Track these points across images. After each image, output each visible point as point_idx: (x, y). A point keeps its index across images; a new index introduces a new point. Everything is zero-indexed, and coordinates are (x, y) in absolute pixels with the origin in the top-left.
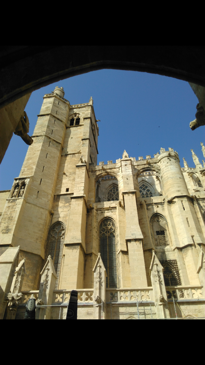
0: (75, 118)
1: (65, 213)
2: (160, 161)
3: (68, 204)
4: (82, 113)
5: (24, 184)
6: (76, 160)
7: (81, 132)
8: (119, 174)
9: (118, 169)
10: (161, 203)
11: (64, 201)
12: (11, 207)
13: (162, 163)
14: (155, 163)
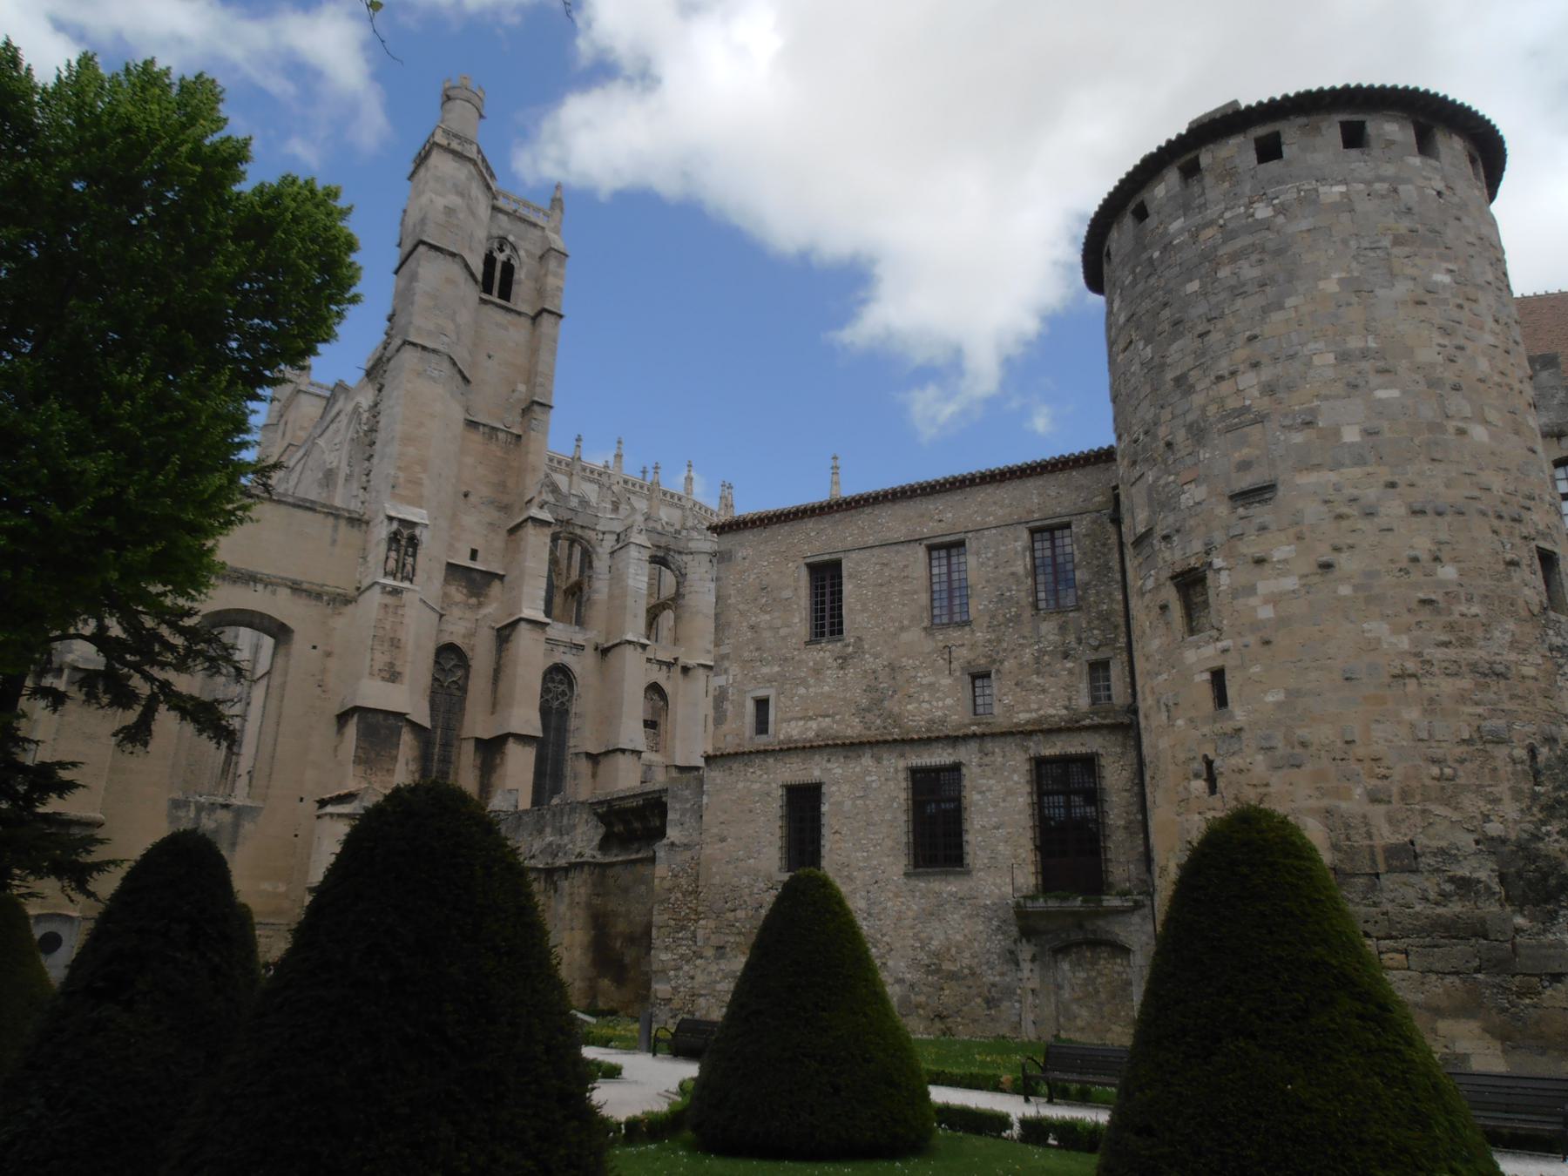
0: (501, 257)
1: (469, 625)
2: (692, 553)
3: (473, 601)
4: (526, 251)
5: (413, 542)
6: (499, 454)
8: (599, 550)
9: (600, 536)
10: (670, 663)
11: (466, 587)
12: (391, 610)
14: (680, 553)
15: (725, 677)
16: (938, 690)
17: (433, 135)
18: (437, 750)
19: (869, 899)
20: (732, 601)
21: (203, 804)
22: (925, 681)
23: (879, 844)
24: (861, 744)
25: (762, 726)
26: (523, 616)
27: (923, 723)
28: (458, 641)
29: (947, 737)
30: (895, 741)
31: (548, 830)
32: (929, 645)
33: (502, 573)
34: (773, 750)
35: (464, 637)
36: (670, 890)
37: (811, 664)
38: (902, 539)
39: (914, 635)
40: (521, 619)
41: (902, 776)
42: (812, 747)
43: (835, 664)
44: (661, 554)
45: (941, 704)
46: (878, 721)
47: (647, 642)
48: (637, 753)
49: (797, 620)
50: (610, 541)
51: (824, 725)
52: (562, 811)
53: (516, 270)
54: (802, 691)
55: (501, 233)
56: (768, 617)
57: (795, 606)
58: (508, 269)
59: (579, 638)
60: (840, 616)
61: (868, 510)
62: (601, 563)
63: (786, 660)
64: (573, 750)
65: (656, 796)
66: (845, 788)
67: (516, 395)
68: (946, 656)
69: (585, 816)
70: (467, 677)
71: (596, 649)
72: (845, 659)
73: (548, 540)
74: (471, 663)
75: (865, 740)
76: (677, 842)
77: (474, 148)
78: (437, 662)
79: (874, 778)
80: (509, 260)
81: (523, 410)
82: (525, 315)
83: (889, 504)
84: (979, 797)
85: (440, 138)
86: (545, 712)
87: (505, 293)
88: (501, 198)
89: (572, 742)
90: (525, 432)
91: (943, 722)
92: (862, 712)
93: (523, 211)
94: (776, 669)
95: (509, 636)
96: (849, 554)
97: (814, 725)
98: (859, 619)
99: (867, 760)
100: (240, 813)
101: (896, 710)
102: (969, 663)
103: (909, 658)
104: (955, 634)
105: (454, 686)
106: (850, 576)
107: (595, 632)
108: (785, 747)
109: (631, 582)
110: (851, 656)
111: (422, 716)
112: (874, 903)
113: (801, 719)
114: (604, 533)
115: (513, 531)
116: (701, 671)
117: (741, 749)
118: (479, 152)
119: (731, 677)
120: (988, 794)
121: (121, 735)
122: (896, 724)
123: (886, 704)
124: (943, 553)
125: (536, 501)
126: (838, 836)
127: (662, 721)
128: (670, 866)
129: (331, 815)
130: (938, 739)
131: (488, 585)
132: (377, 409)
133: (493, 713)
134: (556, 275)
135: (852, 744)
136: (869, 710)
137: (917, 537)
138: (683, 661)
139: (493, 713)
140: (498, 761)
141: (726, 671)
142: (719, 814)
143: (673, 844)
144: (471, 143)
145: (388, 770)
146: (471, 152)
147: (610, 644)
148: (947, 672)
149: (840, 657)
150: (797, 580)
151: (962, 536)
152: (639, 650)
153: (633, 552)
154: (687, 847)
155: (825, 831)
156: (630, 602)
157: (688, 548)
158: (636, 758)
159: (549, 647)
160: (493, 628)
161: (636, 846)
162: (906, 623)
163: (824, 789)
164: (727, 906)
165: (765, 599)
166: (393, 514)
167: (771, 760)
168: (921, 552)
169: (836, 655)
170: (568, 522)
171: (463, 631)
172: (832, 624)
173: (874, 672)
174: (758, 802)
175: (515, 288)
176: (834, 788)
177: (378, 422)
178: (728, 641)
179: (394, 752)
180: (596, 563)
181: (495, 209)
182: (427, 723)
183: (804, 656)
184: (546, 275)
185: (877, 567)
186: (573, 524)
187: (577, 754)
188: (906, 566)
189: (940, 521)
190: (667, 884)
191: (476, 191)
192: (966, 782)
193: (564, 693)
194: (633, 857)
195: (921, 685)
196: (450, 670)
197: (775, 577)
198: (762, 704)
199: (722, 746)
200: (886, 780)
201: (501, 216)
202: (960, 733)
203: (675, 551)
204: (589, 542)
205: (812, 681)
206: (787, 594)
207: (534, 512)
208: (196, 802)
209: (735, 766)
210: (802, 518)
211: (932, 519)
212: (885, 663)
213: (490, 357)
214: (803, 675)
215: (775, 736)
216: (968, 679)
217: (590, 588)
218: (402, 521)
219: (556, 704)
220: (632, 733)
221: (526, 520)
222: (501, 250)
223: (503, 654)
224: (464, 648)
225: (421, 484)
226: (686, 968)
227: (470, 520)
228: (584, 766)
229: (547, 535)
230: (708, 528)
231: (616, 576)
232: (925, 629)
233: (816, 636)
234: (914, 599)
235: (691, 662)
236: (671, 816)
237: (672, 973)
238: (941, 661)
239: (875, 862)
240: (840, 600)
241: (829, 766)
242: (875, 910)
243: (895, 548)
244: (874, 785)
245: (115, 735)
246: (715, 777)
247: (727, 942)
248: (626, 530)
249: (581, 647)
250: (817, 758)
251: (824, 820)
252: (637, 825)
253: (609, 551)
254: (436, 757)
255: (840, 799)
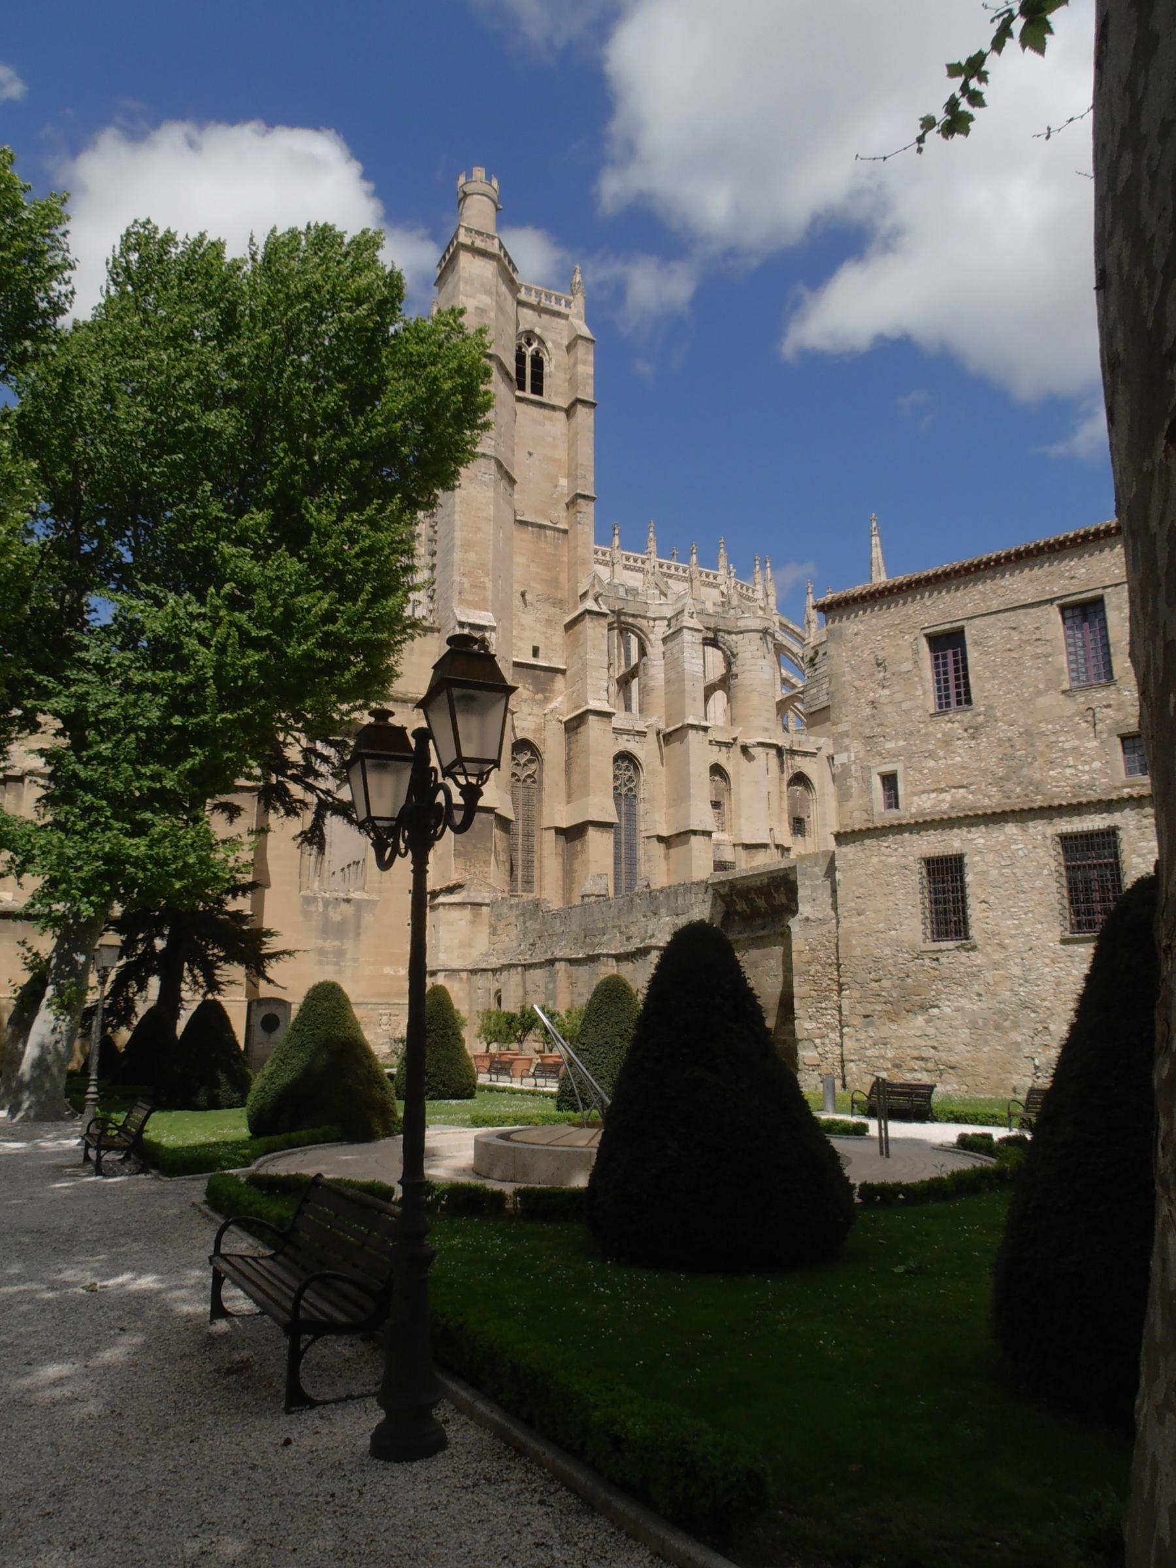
0: (529, 351)
2: (741, 632)
3: (539, 696)
4: (553, 342)
6: (548, 550)
7: (554, 438)
8: (651, 637)
9: (651, 623)
11: (533, 684)
13: (746, 641)
14: (730, 633)
15: (846, 755)
16: (1082, 755)
17: (456, 236)
18: (520, 841)
19: (1024, 966)
20: (847, 678)
21: (328, 899)
22: (1067, 745)
23: (1031, 912)
24: (1004, 812)
25: (893, 801)
26: (590, 707)
27: (1068, 789)
28: (530, 737)
29: (1100, 801)
30: (1041, 808)
31: (663, 911)
32: (1069, 707)
33: (563, 667)
34: (908, 824)
35: (536, 731)
36: (809, 963)
37: (939, 736)
38: (1030, 601)
39: (1051, 700)
40: (589, 711)
41: (1049, 841)
42: (950, 818)
43: (965, 735)
44: (711, 635)
45: (1087, 768)
46: (1018, 789)
47: (704, 723)
48: (708, 834)
49: (919, 693)
50: (661, 629)
51: (959, 796)
52: (676, 892)
53: (545, 364)
54: (931, 763)
55: (528, 327)
56: (887, 692)
57: (916, 679)
58: (538, 363)
59: (640, 727)
60: (967, 685)
61: (989, 574)
62: (656, 649)
63: (911, 733)
64: (644, 834)
65: (781, 874)
66: (990, 857)
67: (559, 489)
68: (1090, 719)
69: (701, 896)
70: (541, 770)
71: (658, 734)
72: (976, 728)
73: (605, 631)
74: (544, 756)
75: (1008, 809)
76: (811, 917)
77: (496, 242)
78: (514, 759)
79: (1020, 846)
80: (537, 353)
81: (567, 505)
82: (560, 409)
83: (1011, 565)
84: (1140, 860)
85: (464, 238)
86: (617, 797)
87: (538, 389)
88: (523, 290)
89: (642, 826)
90: (571, 526)
91: (1091, 786)
92: (998, 781)
93: (544, 303)
94: (902, 743)
95: (578, 726)
96: (970, 621)
97: (947, 797)
98: (988, 686)
99: (1011, 829)
100: (359, 905)
101: (1037, 776)
102: (1117, 723)
103: (1048, 723)
104: (1100, 696)
105: (529, 780)
106: (976, 643)
107: (655, 718)
108: (921, 820)
109: (687, 666)
110: (982, 725)
111: (507, 811)
112: (1030, 970)
113: (933, 791)
114: (654, 619)
115: (569, 626)
116: (760, 749)
117: (871, 826)
118: (501, 246)
119: (853, 755)
120: (1149, 856)
121: (300, 840)
122: (1038, 791)
123: (1025, 771)
124: (1077, 612)
125: (591, 594)
126: (984, 906)
127: (725, 801)
128: (806, 940)
129: (444, 904)
130: (1089, 804)
131: (552, 680)
132: (435, 519)
133: (568, 803)
134: (585, 363)
135: (994, 813)
136: (1006, 778)
137: (1048, 597)
138: (741, 741)
139: (568, 803)
140: (579, 848)
141: (847, 749)
142: (854, 888)
143: (807, 919)
144: (493, 238)
145: (485, 862)
146: (494, 248)
147: (671, 729)
148: (1092, 735)
149: (971, 727)
150: (916, 652)
151: (1100, 592)
152: (702, 733)
153: (687, 635)
154: (822, 921)
155: (970, 901)
156: (688, 686)
157: (738, 627)
158: (707, 838)
159: (614, 736)
160: (560, 721)
161: (759, 922)
162: (1041, 686)
163: (966, 860)
164: (871, 976)
165: (882, 674)
166: (463, 619)
167: (906, 835)
168: (1054, 613)
169: (966, 725)
170: (619, 613)
171: (532, 726)
172: (958, 694)
173: (1010, 740)
174: (892, 876)
175: (546, 382)
176: (977, 858)
177: (435, 532)
178: (845, 719)
179: (488, 845)
180: (649, 650)
181: (521, 303)
182: (511, 815)
183: (931, 729)
184: (575, 364)
185: (1005, 632)
186: (625, 614)
187: (648, 837)
188: (1037, 628)
189: (1073, 578)
190: (806, 956)
191: (504, 289)
192: (1124, 846)
193: (630, 779)
194: (761, 933)
195: (1063, 750)
196: (525, 765)
197: (893, 650)
198: (890, 780)
199: (849, 822)
200: (1035, 847)
201: (527, 313)
202: (1114, 796)
203: (724, 631)
204: (641, 630)
205: (941, 753)
206: (907, 666)
207: (590, 604)
208: (323, 898)
209: (867, 842)
210: (917, 588)
211: (1061, 576)
212: (1022, 730)
213: (530, 454)
214: (931, 747)
215: (906, 810)
216: (1118, 741)
217: (646, 675)
218: (473, 626)
219: (624, 790)
220: (701, 815)
221: (583, 614)
222: (530, 344)
223: (573, 746)
224: (536, 742)
225: (485, 588)
226: (831, 1035)
227: (527, 618)
228: (658, 848)
229: (603, 627)
230: (814, 607)
231: (673, 664)
232: (1064, 692)
233: (940, 706)
234: (1048, 663)
235: (750, 741)
236: (801, 893)
237: (818, 1041)
238: (1084, 725)
239: (1028, 930)
240: (965, 668)
241: (970, 836)
242: (1033, 976)
243: (1023, 611)
244: (1021, 853)
245: (294, 839)
246: (849, 852)
247: (874, 1011)
248: (677, 615)
249: (642, 734)
250: (956, 831)
251: (968, 891)
252: (761, 903)
253: (661, 637)
254: (520, 847)
255: (985, 868)
